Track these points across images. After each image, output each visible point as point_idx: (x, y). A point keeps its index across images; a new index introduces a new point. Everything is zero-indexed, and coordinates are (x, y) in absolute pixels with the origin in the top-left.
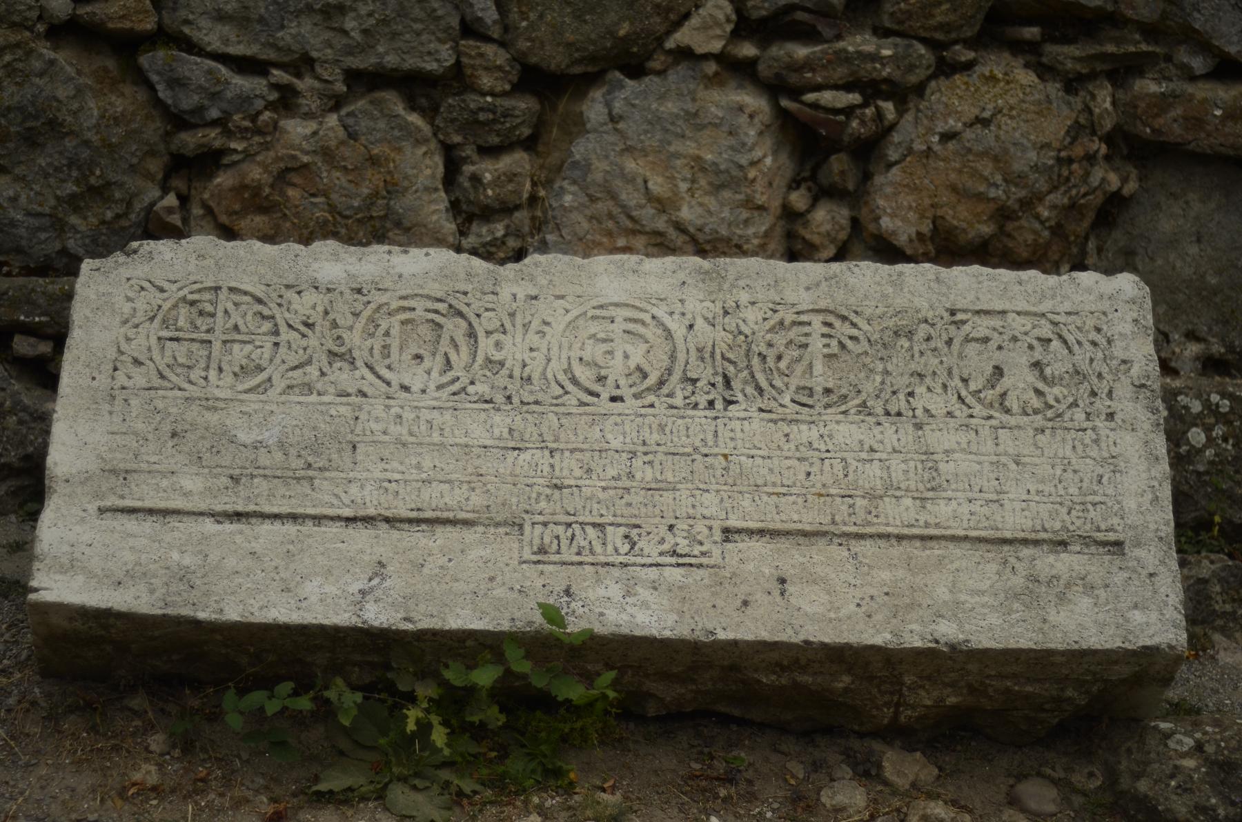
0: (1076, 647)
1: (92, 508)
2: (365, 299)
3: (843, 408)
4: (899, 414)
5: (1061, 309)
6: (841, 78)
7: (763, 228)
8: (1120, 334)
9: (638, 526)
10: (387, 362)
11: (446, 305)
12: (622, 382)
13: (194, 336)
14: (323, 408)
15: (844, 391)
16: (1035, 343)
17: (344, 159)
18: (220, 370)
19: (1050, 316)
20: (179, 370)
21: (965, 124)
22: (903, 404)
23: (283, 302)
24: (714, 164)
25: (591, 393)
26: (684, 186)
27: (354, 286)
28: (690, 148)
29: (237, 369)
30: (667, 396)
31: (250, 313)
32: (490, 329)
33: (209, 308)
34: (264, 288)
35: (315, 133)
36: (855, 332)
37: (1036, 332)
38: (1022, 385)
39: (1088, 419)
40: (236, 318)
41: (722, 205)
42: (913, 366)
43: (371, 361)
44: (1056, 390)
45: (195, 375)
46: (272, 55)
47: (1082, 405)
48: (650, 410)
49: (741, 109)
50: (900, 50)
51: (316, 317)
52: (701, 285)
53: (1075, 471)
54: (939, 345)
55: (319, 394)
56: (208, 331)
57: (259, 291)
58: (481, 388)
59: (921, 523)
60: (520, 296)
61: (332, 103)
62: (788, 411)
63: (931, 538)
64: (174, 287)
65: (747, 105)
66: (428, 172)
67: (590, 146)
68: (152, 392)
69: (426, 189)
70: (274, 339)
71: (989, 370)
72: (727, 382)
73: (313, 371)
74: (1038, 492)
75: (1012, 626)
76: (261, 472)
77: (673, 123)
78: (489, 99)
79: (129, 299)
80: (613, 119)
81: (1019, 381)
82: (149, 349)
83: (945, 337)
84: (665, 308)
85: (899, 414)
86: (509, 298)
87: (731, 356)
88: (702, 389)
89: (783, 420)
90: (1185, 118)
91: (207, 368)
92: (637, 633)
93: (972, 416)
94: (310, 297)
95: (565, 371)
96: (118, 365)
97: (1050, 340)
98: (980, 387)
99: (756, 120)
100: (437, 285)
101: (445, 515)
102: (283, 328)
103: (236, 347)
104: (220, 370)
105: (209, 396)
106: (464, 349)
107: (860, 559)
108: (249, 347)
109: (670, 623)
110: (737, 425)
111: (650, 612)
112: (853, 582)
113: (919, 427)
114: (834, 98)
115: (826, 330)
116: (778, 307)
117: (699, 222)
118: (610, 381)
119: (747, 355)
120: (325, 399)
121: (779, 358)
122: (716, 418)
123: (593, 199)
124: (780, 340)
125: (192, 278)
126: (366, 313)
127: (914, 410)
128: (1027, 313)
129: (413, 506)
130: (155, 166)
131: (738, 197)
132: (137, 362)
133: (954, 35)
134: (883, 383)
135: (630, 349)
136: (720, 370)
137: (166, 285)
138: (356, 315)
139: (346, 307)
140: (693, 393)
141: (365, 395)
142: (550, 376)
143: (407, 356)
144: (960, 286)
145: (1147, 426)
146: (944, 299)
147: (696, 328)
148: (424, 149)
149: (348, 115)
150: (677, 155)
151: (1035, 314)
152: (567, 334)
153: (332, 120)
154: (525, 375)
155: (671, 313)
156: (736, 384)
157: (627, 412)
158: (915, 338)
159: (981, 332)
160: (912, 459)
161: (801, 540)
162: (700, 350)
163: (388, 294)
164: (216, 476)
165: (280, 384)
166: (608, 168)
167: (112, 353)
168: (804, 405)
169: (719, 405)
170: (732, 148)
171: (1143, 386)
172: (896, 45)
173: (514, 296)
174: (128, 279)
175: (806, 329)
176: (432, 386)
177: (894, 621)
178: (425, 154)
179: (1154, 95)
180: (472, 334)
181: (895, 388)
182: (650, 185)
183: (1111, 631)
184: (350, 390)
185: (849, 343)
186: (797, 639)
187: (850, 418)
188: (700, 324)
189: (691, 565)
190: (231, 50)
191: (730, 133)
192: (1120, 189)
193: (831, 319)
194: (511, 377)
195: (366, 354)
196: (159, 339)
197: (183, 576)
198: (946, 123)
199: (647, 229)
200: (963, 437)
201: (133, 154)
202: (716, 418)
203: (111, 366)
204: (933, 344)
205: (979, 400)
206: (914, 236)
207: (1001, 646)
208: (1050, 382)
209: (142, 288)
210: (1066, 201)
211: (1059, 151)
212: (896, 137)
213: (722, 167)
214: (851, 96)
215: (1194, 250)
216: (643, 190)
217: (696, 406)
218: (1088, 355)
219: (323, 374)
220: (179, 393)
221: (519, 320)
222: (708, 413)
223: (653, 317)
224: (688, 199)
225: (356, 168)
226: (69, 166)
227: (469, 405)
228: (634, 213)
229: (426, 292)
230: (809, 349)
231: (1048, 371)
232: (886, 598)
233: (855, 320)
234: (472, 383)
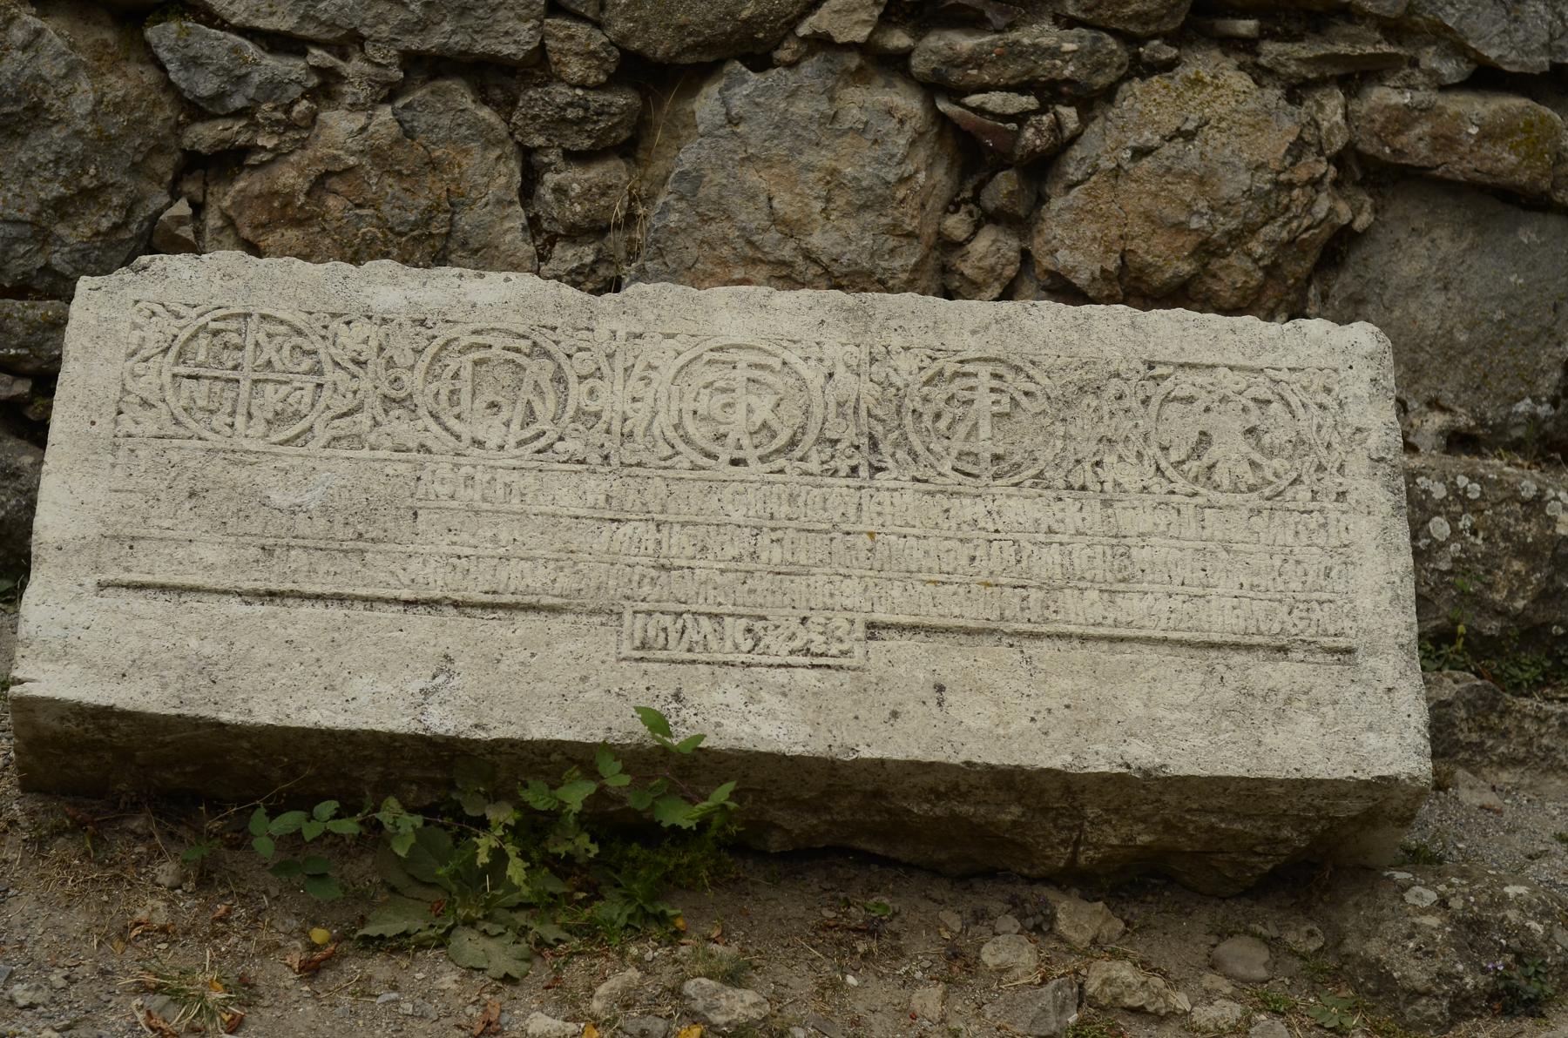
0: (1298, 776)
1: (90, 582)
2: (430, 332)
3: (1016, 479)
4: (1083, 488)
5: (1283, 364)
6: (1013, 78)
7: (913, 261)
8: (1355, 396)
9: (764, 618)
10: (456, 410)
11: (529, 343)
12: (745, 442)
13: (218, 373)
14: (377, 465)
15: (1017, 458)
16: (1251, 404)
17: (400, 163)
18: (250, 416)
19: (1271, 372)
20: (199, 415)
21: (1163, 137)
22: (1089, 474)
23: (329, 335)
24: (855, 178)
25: (708, 455)
26: (818, 206)
27: (416, 316)
28: (824, 159)
29: (270, 416)
30: (801, 459)
31: (287, 347)
32: (584, 373)
33: (235, 339)
34: (304, 316)
35: (363, 129)
36: (1031, 387)
37: (1252, 392)
38: (1234, 456)
39: (1314, 499)
40: (269, 352)
41: (864, 229)
42: (1102, 430)
43: (435, 408)
44: (1276, 463)
45: (219, 421)
46: (310, 30)
47: (1307, 482)
48: (779, 477)
49: (890, 112)
50: (1087, 43)
51: (369, 353)
52: (843, 324)
53: (1298, 562)
55: (372, 449)
56: (235, 368)
57: (299, 320)
58: (570, 445)
59: (1110, 621)
60: (621, 333)
61: (385, 92)
62: (948, 481)
63: (1122, 640)
64: (194, 313)
65: (897, 108)
66: (503, 180)
67: (704, 153)
68: (166, 441)
69: (499, 202)
70: (316, 379)
71: (1195, 437)
72: (874, 445)
73: (364, 419)
74: (1252, 586)
75: (1220, 749)
76: (301, 542)
77: (805, 128)
78: (579, 92)
79: (135, 326)
80: (732, 120)
81: (1230, 450)
82: (161, 388)
83: (1141, 396)
84: (799, 352)
85: (1083, 488)
86: (607, 335)
87: (879, 412)
88: (843, 453)
89: (942, 492)
90: (1435, 138)
91: (233, 413)
92: (762, 748)
94: (362, 329)
95: (676, 427)
96: (123, 407)
97: (1269, 402)
98: (1183, 457)
99: (907, 127)
100: (518, 318)
101: (527, 599)
102: (328, 367)
103: (270, 388)
104: (250, 416)
105: (236, 447)
106: (551, 398)
107: (1036, 663)
108: (284, 389)
109: (801, 737)
110: (884, 496)
111: (778, 723)
112: (1026, 691)
113: (1106, 503)
114: (1004, 101)
115: (995, 383)
116: (938, 354)
117: (836, 250)
118: (730, 440)
119: (898, 412)
120: (380, 454)
121: (938, 416)
122: (860, 488)
123: (705, 220)
124: (939, 394)
125: (216, 303)
126: (432, 350)
128: (1242, 369)
129: (487, 588)
130: (164, 166)
131: (883, 220)
132: (145, 403)
133: (1152, 28)
134: (1064, 450)
135: (753, 399)
136: (866, 430)
137: (183, 310)
138: (419, 352)
139: (407, 342)
140: (833, 457)
141: (429, 451)
142: (656, 431)
143: (480, 404)
144: (1161, 333)
145: (1386, 509)
146: (1140, 349)
147: (836, 377)
148: (498, 152)
149: (406, 107)
150: (809, 168)
151: (1252, 370)
152: (678, 381)
153: (385, 113)
154: (626, 431)
155: (806, 359)
156: (885, 447)
157: (752, 478)
158: (1105, 395)
159: (1186, 390)
160: (1100, 543)
161: (963, 639)
162: (839, 405)
163: (459, 327)
164: (244, 546)
165: (322, 435)
166: (724, 181)
167: (115, 392)
168: (968, 474)
169: (864, 472)
170: (877, 160)
171: (1382, 459)
172: (1081, 38)
173: (614, 333)
174: (137, 302)
175: (972, 382)
176: (512, 441)
177: (1076, 740)
178: (499, 158)
179: (1396, 107)
180: (559, 379)
181: (1080, 456)
182: (775, 203)
183: (1338, 757)
184: (411, 445)
185: (1024, 401)
186: (957, 760)
187: (1025, 491)
188: (840, 371)
189: (829, 667)
190: (260, 23)
191: (875, 142)
192: (1352, 222)
193: (1001, 370)
194: (608, 432)
195: (430, 399)
196: (174, 376)
197: (204, 667)
198: (1141, 136)
199: (771, 258)
200: (1162, 518)
201: (136, 150)
202: (860, 488)
203: (113, 409)
204: (1126, 403)
205: (1184, 474)
206: (1098, 273)
207: (1206, 773)
208: (1271, 453)
209: (154, 313)
210: (1284, 234)
211: (1279, 173)
212: (1077, 152)
213: (865, 184)
214: (1024, 99)
215: (1438, 299)
216: (766, 210)
217: (835, 472)
218: (1315, 421)
219: (376, 424)
220: (196, 443)
221: (619, 364)
222: (850, 481)
223: (784, 363)
224: (822, 222)
225: (413, 173)
226: (57, 162)
227: (557, 466)
228: (755, 238)
229: (504, 326)
230: (975, 406)
231: (1266, 439)
232: (1067, 711)
233: (1031, 373)
234: (561, 439)
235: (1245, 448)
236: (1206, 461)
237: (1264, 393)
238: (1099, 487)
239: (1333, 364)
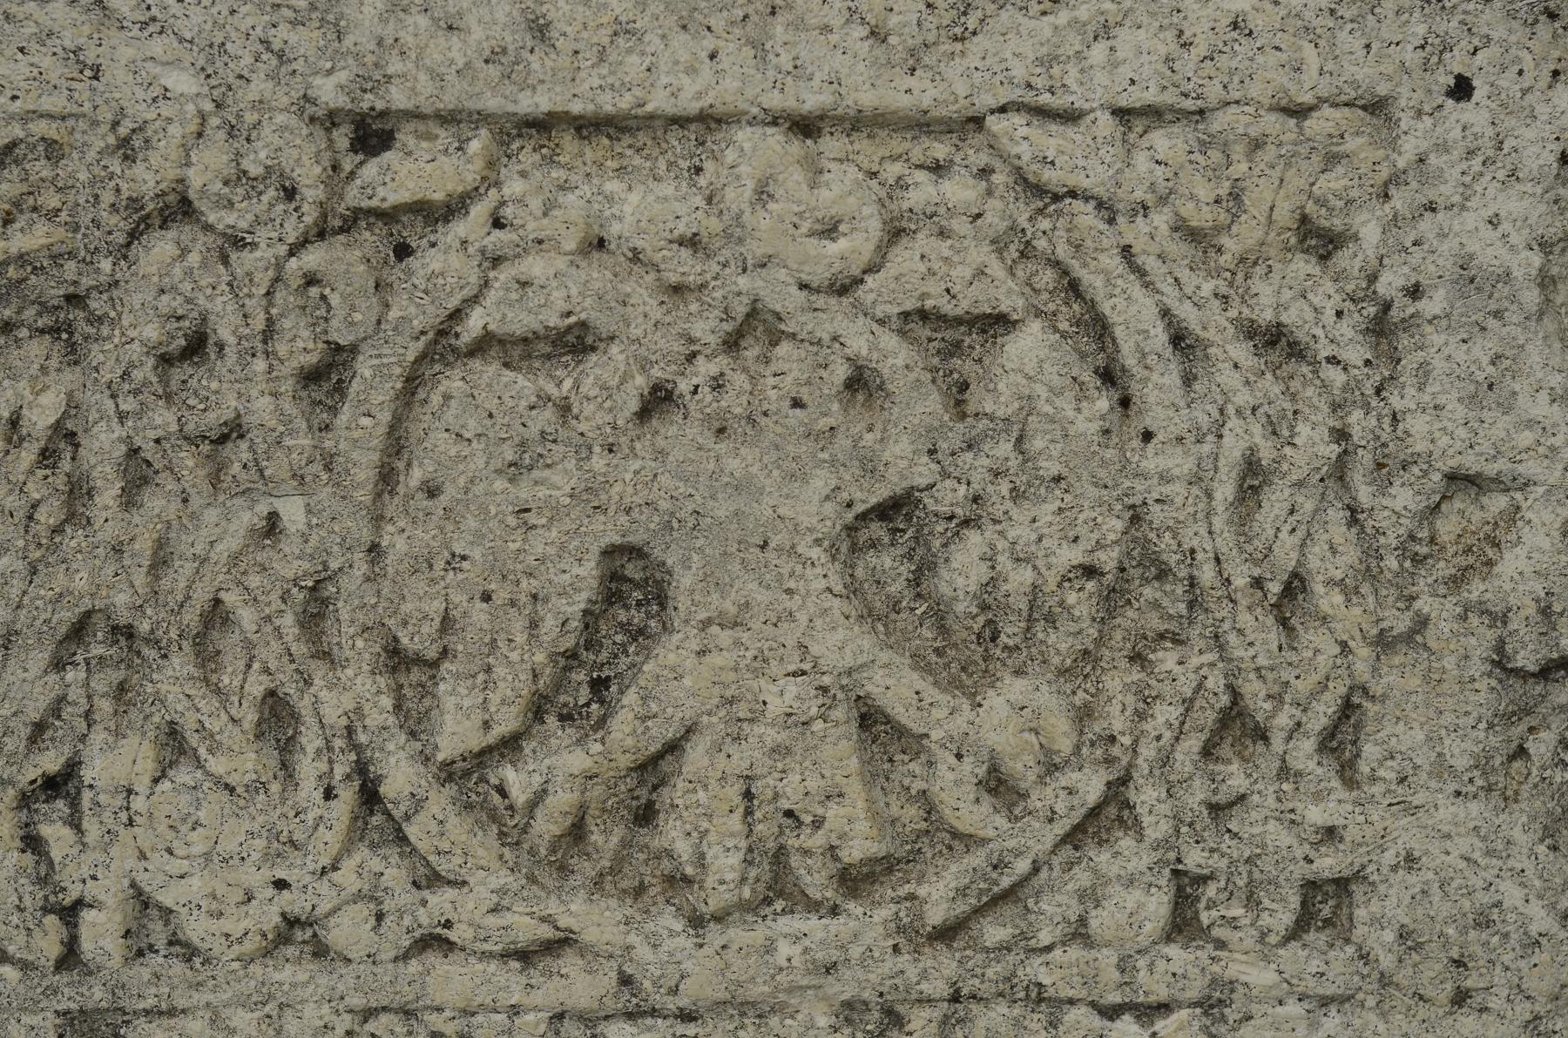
8: (1467, 276)
16: (895, 357)
19: (1022, 138)
37: (911, 274)
38: (783, 695)
39: (1182, 924)
42: (80, 578)
47: (1156, 828)
54: (262, 409)
81: (760, 665)
83: (300, 346)
93: (434, 942)
97: (996, 324)
127: (70, 913)
151: (922, 125)
158: (105, 357)
159: (556, 288)
204: (222, 391)
205: (506, 823)
208: (973, 649)
218: (1233, 449)
231: (963, 570)
235: (842, 643)
236: (628, 732)
237: (968, 274)
238: (49, 944)
239: (1365, 74)
